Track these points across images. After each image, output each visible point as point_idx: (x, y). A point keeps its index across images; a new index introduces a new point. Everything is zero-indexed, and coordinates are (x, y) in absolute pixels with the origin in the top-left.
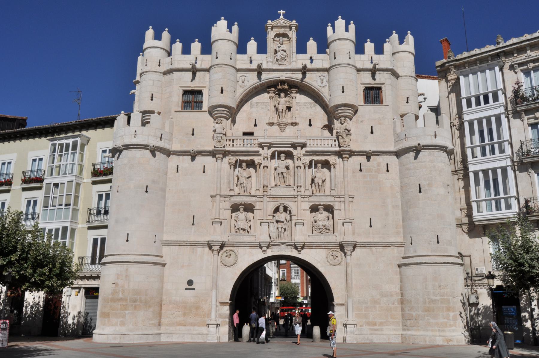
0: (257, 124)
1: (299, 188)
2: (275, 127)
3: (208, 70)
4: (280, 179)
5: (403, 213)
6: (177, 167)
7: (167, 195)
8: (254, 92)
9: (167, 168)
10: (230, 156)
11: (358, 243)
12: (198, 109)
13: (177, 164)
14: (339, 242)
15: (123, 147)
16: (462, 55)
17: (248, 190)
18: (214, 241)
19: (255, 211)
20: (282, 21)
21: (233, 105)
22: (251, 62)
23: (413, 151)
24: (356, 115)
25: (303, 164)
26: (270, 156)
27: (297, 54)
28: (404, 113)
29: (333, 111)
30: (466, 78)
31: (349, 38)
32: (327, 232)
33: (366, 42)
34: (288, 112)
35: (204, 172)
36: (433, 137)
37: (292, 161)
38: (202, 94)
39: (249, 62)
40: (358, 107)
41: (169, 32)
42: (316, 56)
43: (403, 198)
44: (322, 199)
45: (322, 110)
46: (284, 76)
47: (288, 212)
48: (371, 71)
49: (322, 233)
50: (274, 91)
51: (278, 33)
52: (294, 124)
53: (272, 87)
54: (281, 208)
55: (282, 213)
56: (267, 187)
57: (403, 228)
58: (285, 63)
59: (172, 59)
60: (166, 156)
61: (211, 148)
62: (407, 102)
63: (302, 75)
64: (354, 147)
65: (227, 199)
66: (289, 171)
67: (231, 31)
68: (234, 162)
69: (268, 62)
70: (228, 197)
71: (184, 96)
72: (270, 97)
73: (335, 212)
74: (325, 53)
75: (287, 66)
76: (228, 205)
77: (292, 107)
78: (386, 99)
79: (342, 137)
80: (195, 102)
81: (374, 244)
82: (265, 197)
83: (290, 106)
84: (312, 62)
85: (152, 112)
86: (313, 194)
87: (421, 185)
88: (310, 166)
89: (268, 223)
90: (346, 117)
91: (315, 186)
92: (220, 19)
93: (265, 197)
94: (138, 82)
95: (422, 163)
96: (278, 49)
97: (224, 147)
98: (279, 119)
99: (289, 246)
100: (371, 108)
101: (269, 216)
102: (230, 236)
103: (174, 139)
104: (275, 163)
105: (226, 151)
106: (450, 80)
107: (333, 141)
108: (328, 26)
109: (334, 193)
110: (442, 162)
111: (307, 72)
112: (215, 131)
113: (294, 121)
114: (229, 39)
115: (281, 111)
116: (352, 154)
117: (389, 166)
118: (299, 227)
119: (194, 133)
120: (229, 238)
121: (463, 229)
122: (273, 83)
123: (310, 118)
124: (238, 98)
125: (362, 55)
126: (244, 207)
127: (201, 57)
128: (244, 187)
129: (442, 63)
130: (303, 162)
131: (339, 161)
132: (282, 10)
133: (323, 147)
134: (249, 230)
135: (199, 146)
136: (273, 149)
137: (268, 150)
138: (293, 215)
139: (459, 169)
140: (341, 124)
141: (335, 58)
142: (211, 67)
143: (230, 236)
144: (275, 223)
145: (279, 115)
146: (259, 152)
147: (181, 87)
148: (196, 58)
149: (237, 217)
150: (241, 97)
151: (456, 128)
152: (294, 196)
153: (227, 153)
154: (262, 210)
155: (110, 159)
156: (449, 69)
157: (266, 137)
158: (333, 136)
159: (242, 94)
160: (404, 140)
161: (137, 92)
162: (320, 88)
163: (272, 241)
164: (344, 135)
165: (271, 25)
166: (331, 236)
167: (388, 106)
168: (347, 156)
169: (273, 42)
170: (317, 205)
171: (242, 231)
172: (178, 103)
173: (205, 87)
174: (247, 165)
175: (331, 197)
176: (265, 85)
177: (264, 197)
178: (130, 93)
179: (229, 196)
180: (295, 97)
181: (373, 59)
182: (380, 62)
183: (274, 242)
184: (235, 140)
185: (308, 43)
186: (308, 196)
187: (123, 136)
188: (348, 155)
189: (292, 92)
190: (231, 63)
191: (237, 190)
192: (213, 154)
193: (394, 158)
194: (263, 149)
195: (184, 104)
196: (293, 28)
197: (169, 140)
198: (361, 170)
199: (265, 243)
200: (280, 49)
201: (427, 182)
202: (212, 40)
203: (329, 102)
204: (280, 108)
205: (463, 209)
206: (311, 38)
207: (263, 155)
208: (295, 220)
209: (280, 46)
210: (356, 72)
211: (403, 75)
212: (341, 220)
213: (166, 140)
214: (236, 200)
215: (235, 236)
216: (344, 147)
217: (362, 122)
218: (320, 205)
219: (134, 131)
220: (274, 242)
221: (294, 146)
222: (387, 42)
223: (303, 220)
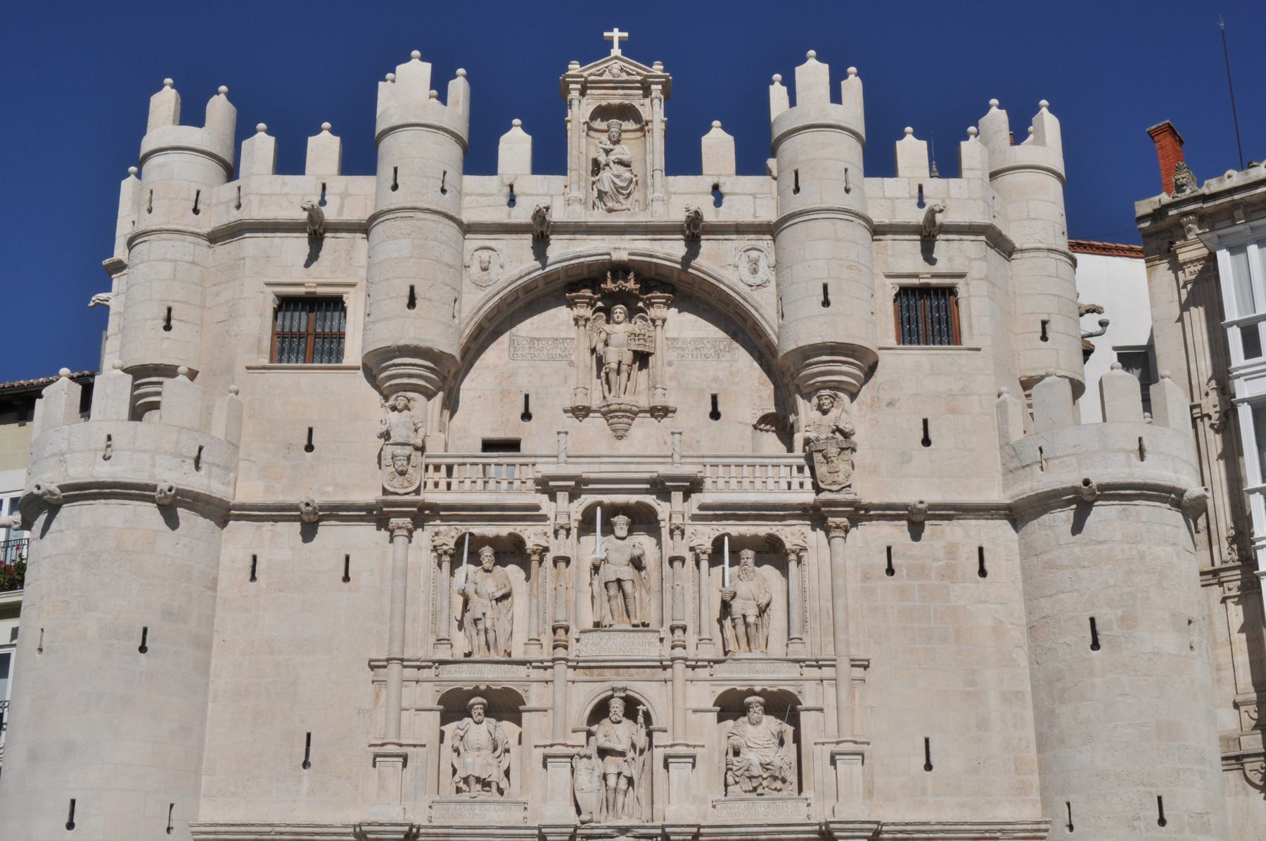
0: (531, 409)
1: (678, 633)
2: (596, 423)
3: (364, 228)
4: (613, 603)
5: (1038, 720)
6: (251, 563)
7: (214, 662)
8: (522, 303)
9: (217, 564)
10: (438, 522)
11: (885, 828)
12: (329, 361)
13: (251, 552)
14: (819, 824)
15: (62, 492)
16: (1221, 181)
17: (501, 641)
18: (381, 825)
19: (525, 716)
20: (616, 64)
21: (450, 345)
22: (512, 202)
23: (1069, 503)
24: (873, 379)
25: (692, 549)
26: (576, 524)
27: (666, 175)
28: (1032, 374)
29: (792, 370)
30: (1238, 256)
31: (842, 124)
32: (776, 789)
33: (902, 136)
34: (640, 369)
35: (346, 578)
36: (1134, 457)
37: (654, 541)
38: (344, 310)
39: (505, 200)
40: (881, 354)
41: (230, 97)
42: (733, 184)
43: (1036, 666)
44: (757, 672)
45: (756, 365)
46: (625, 249)
47: (641, 719)
48: (921, 235)
49: (760, 791)
50: (590, 298)
51: (604, 103)
52: (659, 412)
53: (585, 287)
54: (617, 706)
55: (619, 722)
56: (567, 630)
57: (1040, 774)
58: (627, 204)
59: (239, 188)
60: (212, 523)
61: (371, 496)
62: (1044, 338)
63: (686, 245)
64: (866, 491)
65: (425, 673)
66: (643, 573)
67: (443, 98)
68: (452, 545)
69: (568, 203)
70: (430, 667)
71: (280, 315)
72: (576, 321)
73: (804, 717)
74: (764, 171)
75: (636, 213)
76: (429, 695)
77: (649, 354)
78: (970, 326)
79: (825, 457)
80: (317, 336)
81: (942, 831)
82: (560, 667)
83: (646, 350)
84: (718, 203)
85: (169, 371)
86: (726, 653)
87: (1097, 622)
88: (716, 558)
89: (572, 757)
90: (837, 387)
91: (734, 627)
92: (408, 58)
93: (560, 667)
94: (120, 266)
95: (1099, 547)
96: (602, 158)
97: (417, 492)
98: (607, 394)
100: (920, 357)
101: (573, 732)
102: (435, 806)
103: (242, 465)
104: (594, 546)
105: (423, 506)
106: (1185, 263)
107: (795, 468)
108: (772, 83)
109: (798, 651)
110: (1165, 541)
111: (703, 237)
112: (386, 435)
113: (658, 401)
114: (436, 123)
115: (614, 366)
116: (859, 513)
117: (986, 554)
118: (679, 771)
119: (313, 443)
120: (433, 813)
121: (1247, 772)
122: (585, 272)
123: (714, 392)
124: (468, 324)
125: (887, 181)
126: (485, 701)
127: (339, 184)
128: (486, 631)
129: (1157, 206)
130: (692, 544)
131: (816, 538)
132: (616, 30)
133: (758, 491)
134: (504, 784)
135: (330, 489)
136: (587, 500)
137: (571, 501)
138: (659, 730)
139: (1224, 566)
140: (819, 413)
141: (797, 190)
142: (374, 217)
143: (435, 806)
144: (596, 760)
145: (608, 382)
146: (537, 508)
147: (268, 284)
148: (324, 186)
149: (462, 738)
150: (475, 319)
151: (1212, 426)
152: (661, 661)
153: (427, 512)
154: (551, 712)
155: (14, 535)
156: (1182, 226)
157: (563, 457)
158: (795, 454)
159: (480, 309)
160: (1037, 468)
161: (115, 298)
162: (748, 289)
163: (583, 823)
164: (833, 451)
165: (581, 76)
166: (790, 804)
167: (979, 350)
168: (843, 521)
169: (587, 135)
170: (742, 692)
171: (479, 787)
172: (260, 341)
173: (353, 285)
174: (496, 554)
175: (790, 664)
176: (558, 278)
177: (556, 667)
178: (92, 304)
179: (434, 662)
180: (664, 321)
181: (925, 192)
182: (947, 201)
183: (593, 824)
184: (456, 468)
185: (706, 140)
186: (709, 661)
187: (63, 455)
188: (845, 519)
189: (652, 304)
190: (445, 204)
191: (461, 643)
192: (378, 515)
193: (1004, 526)
194: (553, 498)
195: (278, 345)
196: (653, 87)
197: (227, 469)
198: (890, 571)
199: (558, 830)
200: (612, 157)
201: (1119, 612)
202: (380, 126)
203: (778, 339)
204: (612, 357)
205: (1245, 703)
206: (716, 123)
207: (552, 519)
208: (665, 747)
209: (611, 146)
210: (867, 235)
211: (1025, 246)
212: (826, 747)
213: (215, 469)
214: (458, 676)
215: (453, 805)
216: (830, 491)
217: (890, 404)
218: (751, 692)
219: (105, 437)
220: (593, 824)
221: (661, 488)
222: (972, 137)
223: (694, 746)
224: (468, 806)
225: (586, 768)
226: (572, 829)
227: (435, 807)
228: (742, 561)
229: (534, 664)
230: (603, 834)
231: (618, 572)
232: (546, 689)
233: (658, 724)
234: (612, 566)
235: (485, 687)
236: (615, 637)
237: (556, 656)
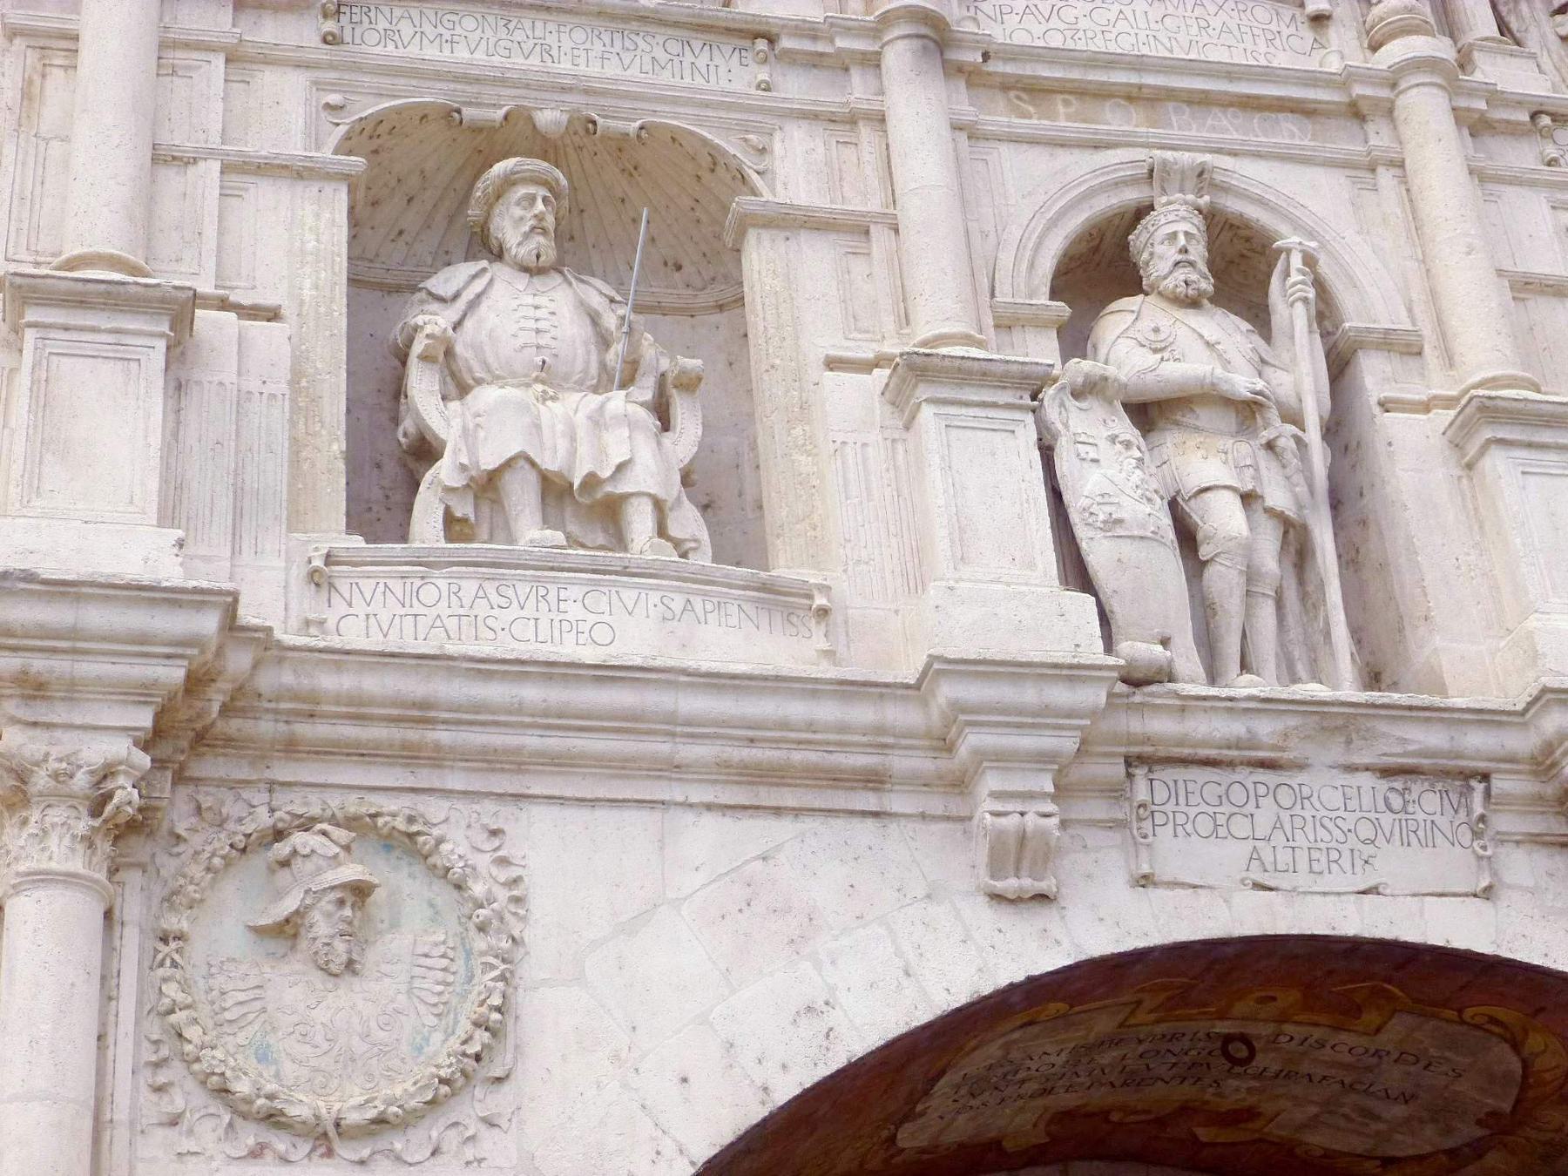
55: (1193, 303)
99: (1429, 801)
199: (1029, 695)
224: (523, 588)
227: (343, 586)
229: (786, 43)
230: (1238, 745)
232: (849, 153)
235: (565, 117)
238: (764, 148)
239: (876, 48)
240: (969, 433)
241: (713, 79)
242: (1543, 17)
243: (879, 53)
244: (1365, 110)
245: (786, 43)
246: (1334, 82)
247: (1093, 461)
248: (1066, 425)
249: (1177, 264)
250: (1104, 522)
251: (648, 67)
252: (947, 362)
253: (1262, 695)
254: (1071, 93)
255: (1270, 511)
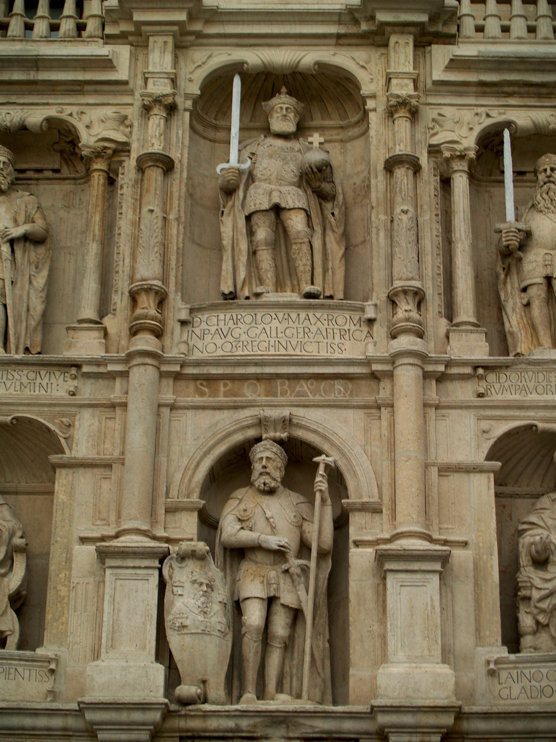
26: (189, 104)
55: (271, 492)
89: (163, 557)
130: (434, 141)
138: (365, 508)
152: (368, 362)
163: (185, 702)
183: (207, 707)
199: (124, 716)
220: (207, 707)
223: (446, 543)
225: (194, 582)
226: (156, 716)
228: (542, 177)
229: (85, 369)
230: (231, 731)
231: (275, 194)
232: (110, 423)
233: (361, 497)
234: (265, 186)
236: (267, 319)
237: (133, 349)
238: (70, 425)
239: (127, 369)
240: (127, 582)
241: (49, 390)
242: (517, 292)
243: (128, 372)
244: (379, 376)
245: (85, 369)
246: (364, 363)
247: (180, 595)
248: (171, 577)
249: (261, 474)
250: (178, 627)
251: (18, 388)
252: (116, 549)
253: (242, 709)
254: (228, 379)
255: (283, 605)
